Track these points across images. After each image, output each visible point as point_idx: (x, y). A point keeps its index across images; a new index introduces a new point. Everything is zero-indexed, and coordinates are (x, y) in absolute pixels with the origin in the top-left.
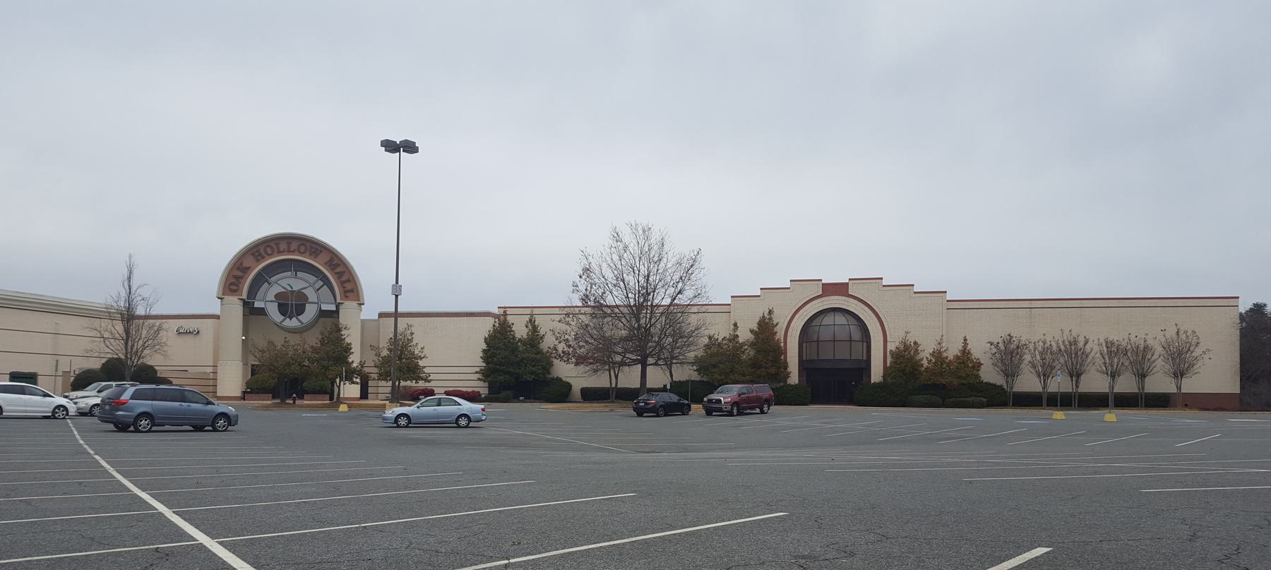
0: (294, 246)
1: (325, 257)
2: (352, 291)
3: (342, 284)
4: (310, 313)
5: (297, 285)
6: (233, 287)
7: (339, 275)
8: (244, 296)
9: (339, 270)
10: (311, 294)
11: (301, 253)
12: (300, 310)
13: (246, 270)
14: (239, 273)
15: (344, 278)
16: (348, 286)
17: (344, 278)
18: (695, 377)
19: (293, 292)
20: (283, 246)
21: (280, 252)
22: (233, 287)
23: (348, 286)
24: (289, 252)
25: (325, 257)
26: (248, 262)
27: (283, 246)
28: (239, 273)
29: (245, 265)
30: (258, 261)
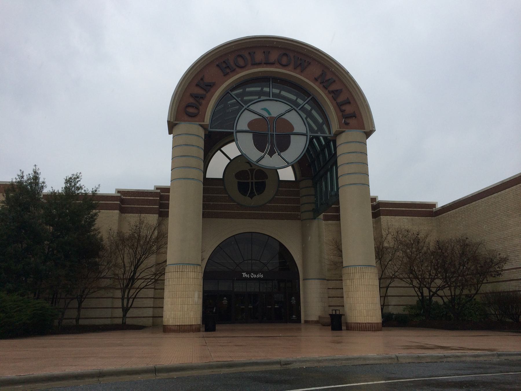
0: (274, 56)
2: (353, 116)
3: (339, 106)
6: (191, 110)
7: (335, 94)
9: (333, 87)
11: (284, 66)
12: (261, 187)
13: (209, 87)
14: (198, 91)
15: (341, 98)
16: (348, 109)
17: (341, 99)
18: (406, 312)
20: (259, 56)
21: (255, 64)
22: (191, 110)
23: (348, 109)
25: (315, 70)
27: (259, 56)
28: (198, 91)
30: (226, 75)
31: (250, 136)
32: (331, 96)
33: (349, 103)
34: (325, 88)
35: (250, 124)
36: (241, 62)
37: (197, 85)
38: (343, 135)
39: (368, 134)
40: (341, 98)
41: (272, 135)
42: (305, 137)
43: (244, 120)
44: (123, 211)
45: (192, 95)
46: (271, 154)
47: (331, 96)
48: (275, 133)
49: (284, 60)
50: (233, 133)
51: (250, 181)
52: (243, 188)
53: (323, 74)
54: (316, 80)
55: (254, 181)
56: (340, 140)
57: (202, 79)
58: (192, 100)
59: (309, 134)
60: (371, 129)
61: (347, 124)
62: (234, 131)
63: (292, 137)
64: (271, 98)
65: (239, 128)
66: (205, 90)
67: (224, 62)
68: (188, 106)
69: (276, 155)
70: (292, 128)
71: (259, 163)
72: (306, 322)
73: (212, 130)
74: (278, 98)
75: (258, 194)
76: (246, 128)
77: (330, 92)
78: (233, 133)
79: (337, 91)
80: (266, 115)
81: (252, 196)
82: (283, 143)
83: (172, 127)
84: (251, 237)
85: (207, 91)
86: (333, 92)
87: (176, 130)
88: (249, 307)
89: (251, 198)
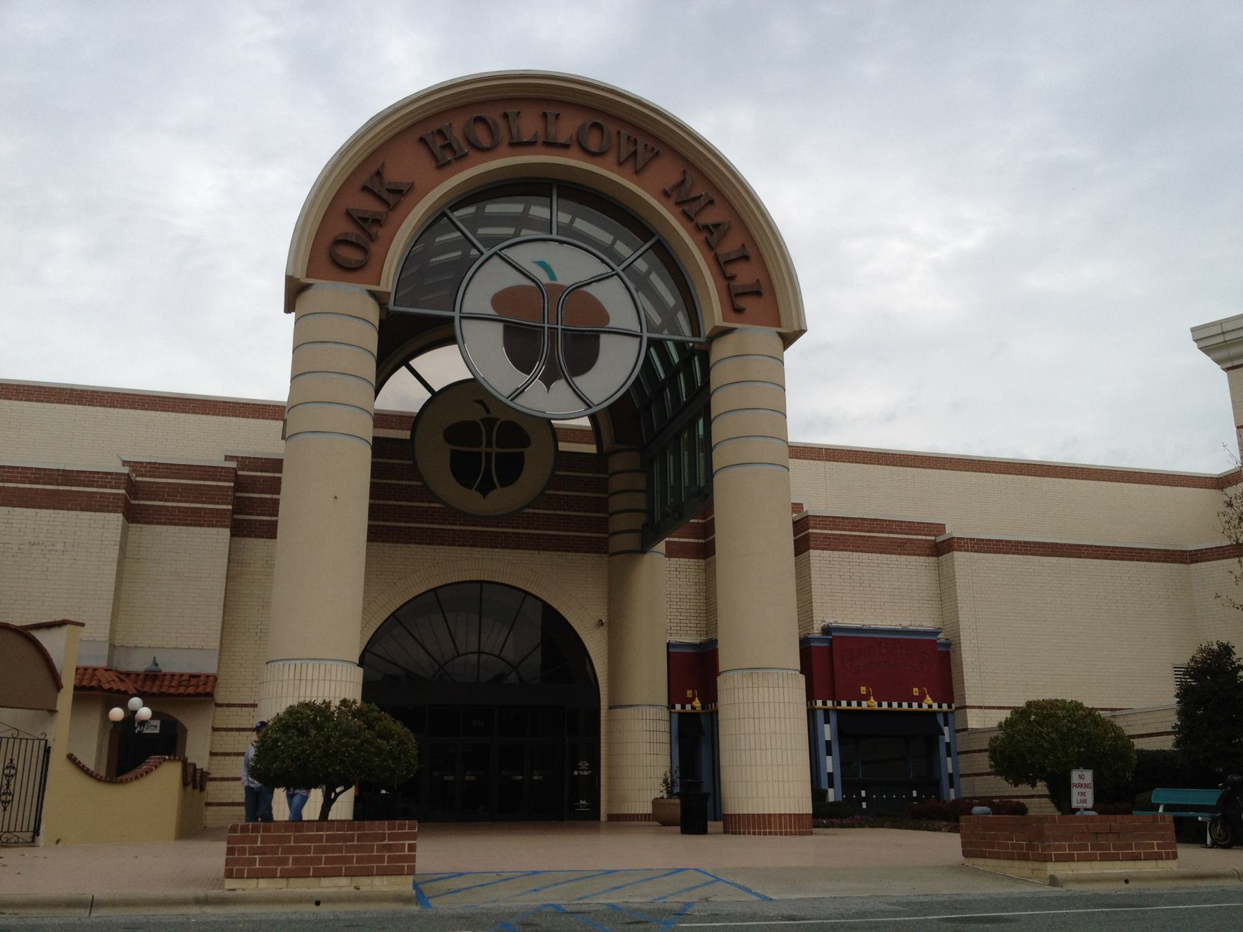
1: (666, 172)
3: (722, 266)
4: (613, 370)
5: (570, 266)
7: (710, 235)
8: (387, 284)
9: (709, 217)
10: (615, 300)
12: (511, 469)
14: (369, 205)
15: (730, 246)
16: (744, 275)
19: (556, 290)
21: (517, 145)
23: (744, 275)
24: (552, 145)
25: (666, 172)
26: (408, 164)
28: (369, 205)
29: (393, 175)
30: (441, 165)
31: (497, 330)
32: (702, 237)
33: (746, 258)
34: (687, 217)
35: (500, 300)
36: (485, 140)
37: (365, 189)
38: (730, 339)
39: (788, 339)
40: (730, 246)
41: (553, 331)
42: (637, 341)
43: (481, 291)
44: (134, 515)
45: (349, 214)
46: (548, 380)
47: (702, 237)
48: (560, 327)
49: (594, 142)
50: (452, 319)
51: (483, 449)
52: (466, 469)
54: (666, 194)
55: (495, 450)
56: (720, 350)
57: (378, 173)
59: (646, 335)
60: (796, 328)
61: (739, 310)
62: (457, 315)
63: (604, 339)
64: (554, 236)
65: (468, 308)
66: (386, 203)
67: (440, 132)
68: (339, 242)
69: (560, 385)
70: (605, 317)
71: (516, 401)
72: (615, 818)
73: (396, 308)
74: (570, 237)
75: (502, 486)
76: (490, 311)
77: (700, 229)
78: (452, 319)
79: (717, 226)
80: (544, 278)
81: (485, 489)
82: (581, 352)
83: (294, 293)
84: (476, 597)
85: (391, 207)
86: (706, 227)
87: (307, 301)
88: (467, 778)
89: (484, 496)
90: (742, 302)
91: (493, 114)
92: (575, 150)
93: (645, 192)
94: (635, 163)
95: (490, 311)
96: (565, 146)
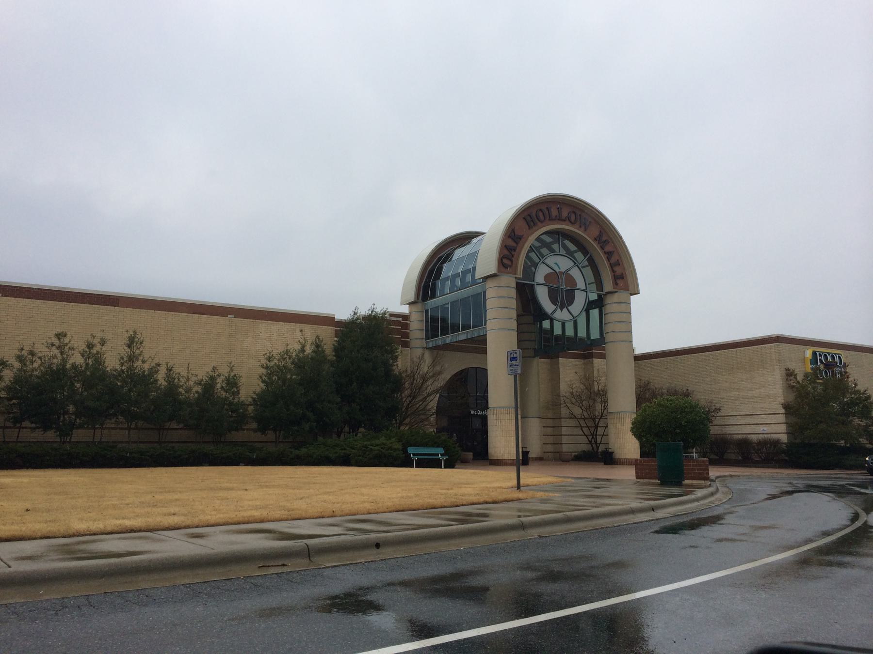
1: (595, 231)
7: (609, 255)
11: (572, 223)
14: (511, 243)
15: (613, 260)
16: (618, 270)
28: (511, 243)
34: (602, 248)
35: (547, 277)
40: (613, 260)
41: (562, 290)
53: (600, 236)
56: (609, 300)
58: (506, 252)
70: (576, 284)
74: (570, 254)
76: (543, 282)
77: (605, 253)
78: (533, 286)
80: (558, 270)
90: (619, 281)
91: (544, 208)
92: (567, 222)
93: (588, 237)
94: (585, 227)
95: (543, 282)
96: (565, 220)
